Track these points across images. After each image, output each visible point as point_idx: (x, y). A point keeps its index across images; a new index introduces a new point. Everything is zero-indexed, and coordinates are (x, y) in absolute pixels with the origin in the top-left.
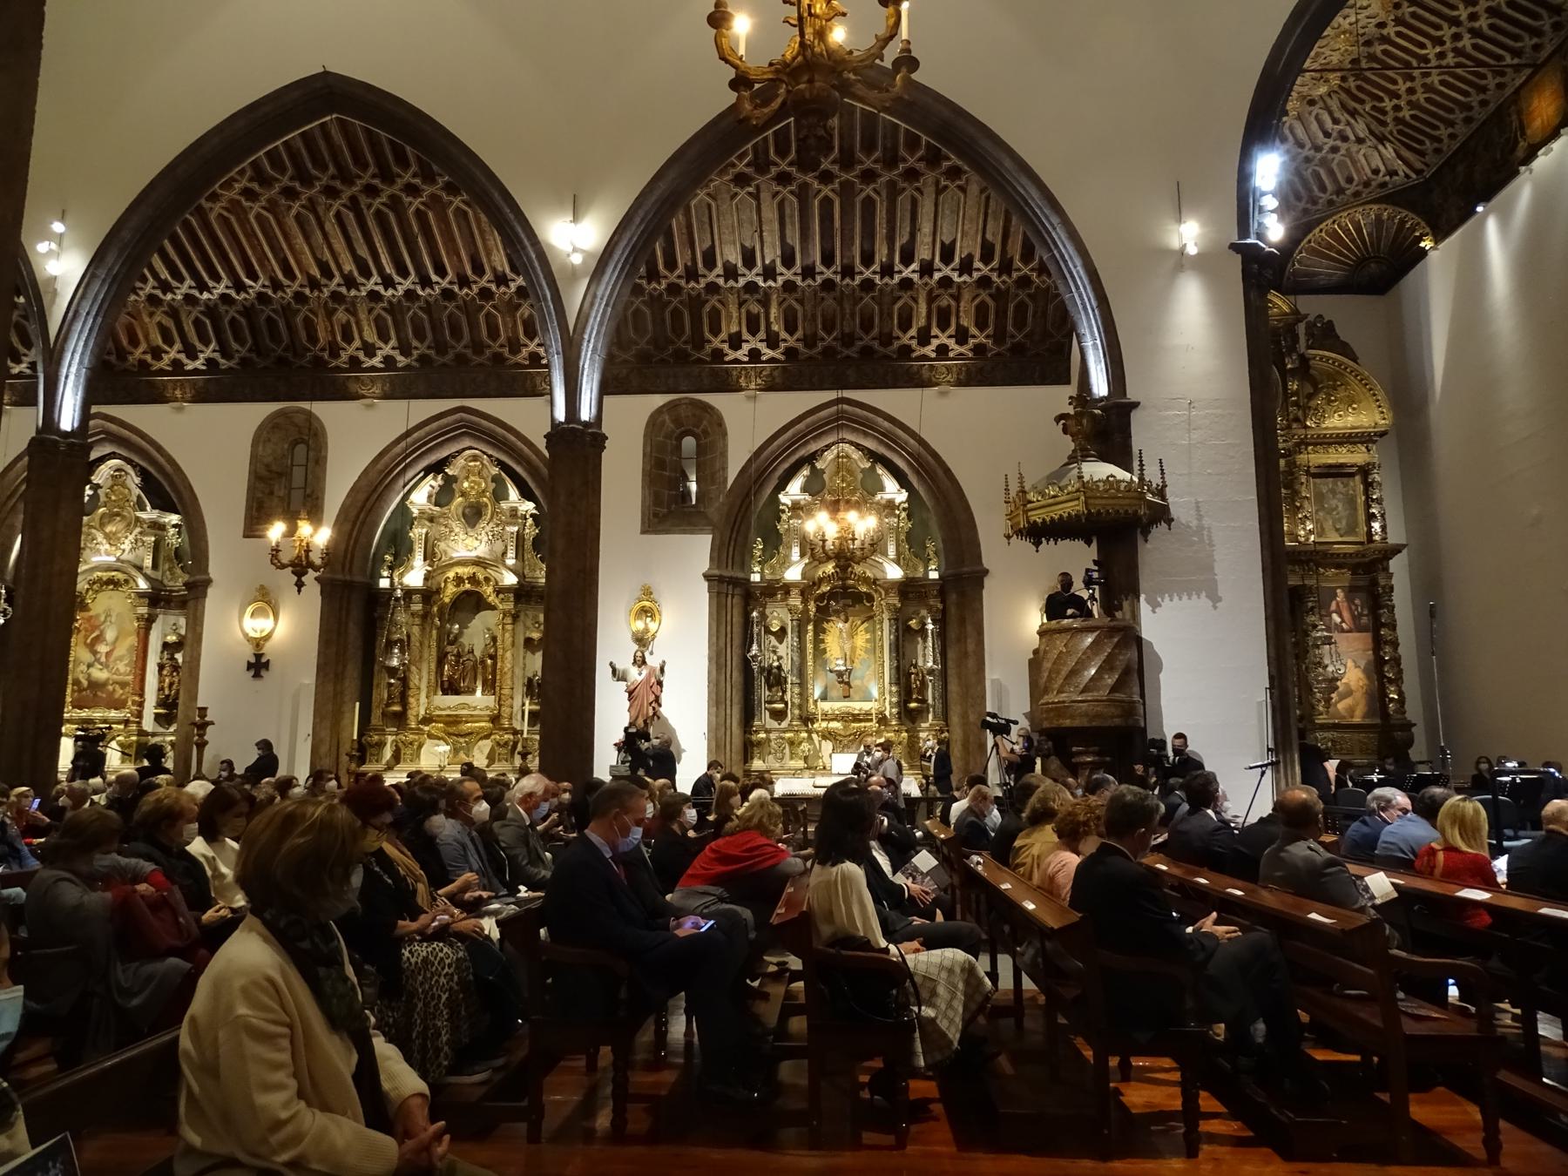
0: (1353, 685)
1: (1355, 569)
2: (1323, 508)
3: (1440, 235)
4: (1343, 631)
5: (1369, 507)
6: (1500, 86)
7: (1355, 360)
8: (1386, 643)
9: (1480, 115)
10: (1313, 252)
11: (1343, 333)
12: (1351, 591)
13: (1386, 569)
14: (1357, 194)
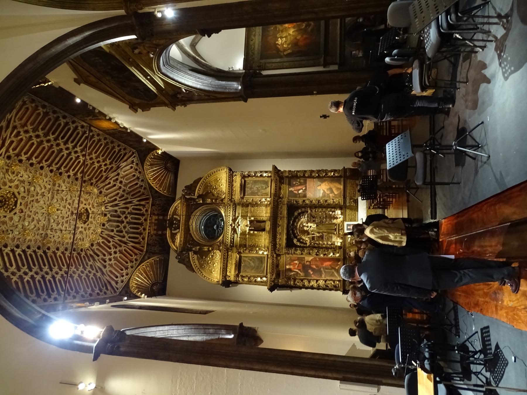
0: (328, 187)
1: (281, 183)
2: (257, 193)
3: (156, 148)
4: (306, 189)
5: (257, 177)
6: (98, 135)
7: (201, 179)
8: (311, 175)
9: (109, 139)
10: (160, 186)
11: (190, 182)
12: (290, 185)
13: (282, 173)
14: (140, 172)
